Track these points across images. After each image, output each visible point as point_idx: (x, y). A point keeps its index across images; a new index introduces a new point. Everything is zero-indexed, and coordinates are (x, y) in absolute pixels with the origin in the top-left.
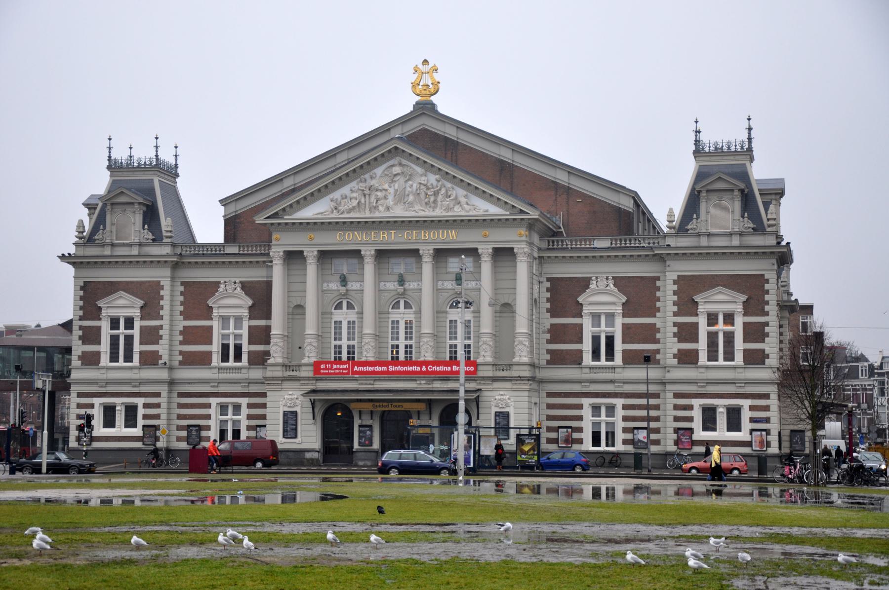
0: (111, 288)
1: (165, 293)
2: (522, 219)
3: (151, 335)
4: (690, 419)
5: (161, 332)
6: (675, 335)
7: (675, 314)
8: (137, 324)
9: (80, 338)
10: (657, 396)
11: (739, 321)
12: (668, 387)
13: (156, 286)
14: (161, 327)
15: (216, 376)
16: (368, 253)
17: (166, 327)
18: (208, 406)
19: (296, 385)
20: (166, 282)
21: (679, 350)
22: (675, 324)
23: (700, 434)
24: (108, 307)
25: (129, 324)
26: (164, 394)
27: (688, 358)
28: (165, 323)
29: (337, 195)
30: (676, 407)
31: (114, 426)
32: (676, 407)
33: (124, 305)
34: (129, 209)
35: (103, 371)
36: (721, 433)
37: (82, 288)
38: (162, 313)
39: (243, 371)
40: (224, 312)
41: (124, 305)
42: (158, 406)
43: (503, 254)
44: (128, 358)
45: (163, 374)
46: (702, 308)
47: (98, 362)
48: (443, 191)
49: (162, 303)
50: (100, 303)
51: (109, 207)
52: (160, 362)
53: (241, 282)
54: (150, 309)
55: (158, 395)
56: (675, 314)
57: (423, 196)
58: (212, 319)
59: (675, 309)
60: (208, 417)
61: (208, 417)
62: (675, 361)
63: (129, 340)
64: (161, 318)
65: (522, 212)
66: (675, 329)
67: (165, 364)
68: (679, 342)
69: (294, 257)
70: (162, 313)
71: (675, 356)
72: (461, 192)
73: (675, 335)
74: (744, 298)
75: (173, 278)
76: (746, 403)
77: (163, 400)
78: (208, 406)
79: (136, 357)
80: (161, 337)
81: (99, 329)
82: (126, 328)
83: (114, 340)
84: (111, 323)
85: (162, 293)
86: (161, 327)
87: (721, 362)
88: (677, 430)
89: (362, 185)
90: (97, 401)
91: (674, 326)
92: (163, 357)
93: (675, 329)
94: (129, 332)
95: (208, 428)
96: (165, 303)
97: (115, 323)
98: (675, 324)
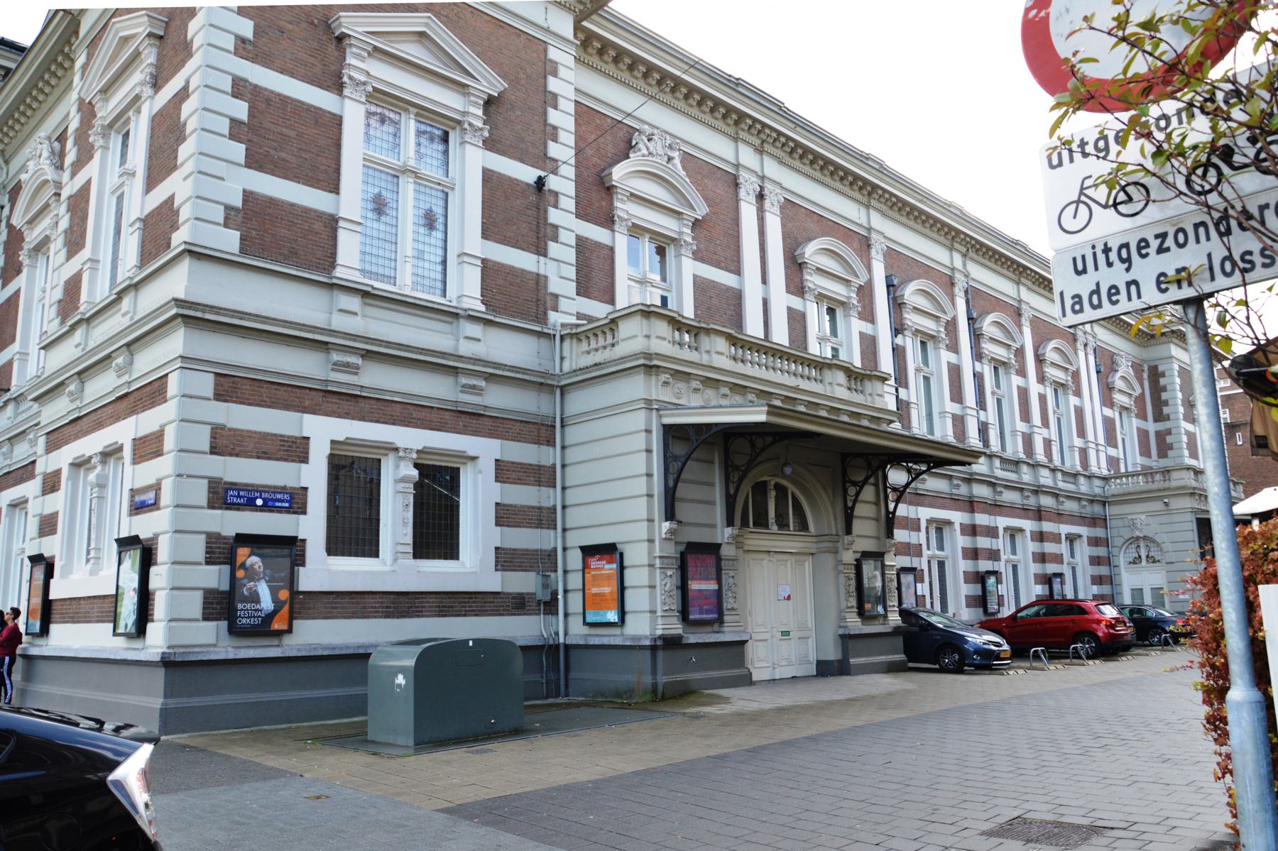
4: (295, 502)
6: (237, 130)
7: (243, 48)
21: (248, 196)
22: (240, 88)
23: (324, 571)
32: (224, 442)
36: (392, 565)
56: (243, 48)
62: (229, 241)
66: (241, 110)
68: (254, 162)
71: (231, 217)
73: (237, 130)
74: (489, 82)
76: (487, 449)
88: (222, 551)
91: (236, 94)
93: (241, 110)
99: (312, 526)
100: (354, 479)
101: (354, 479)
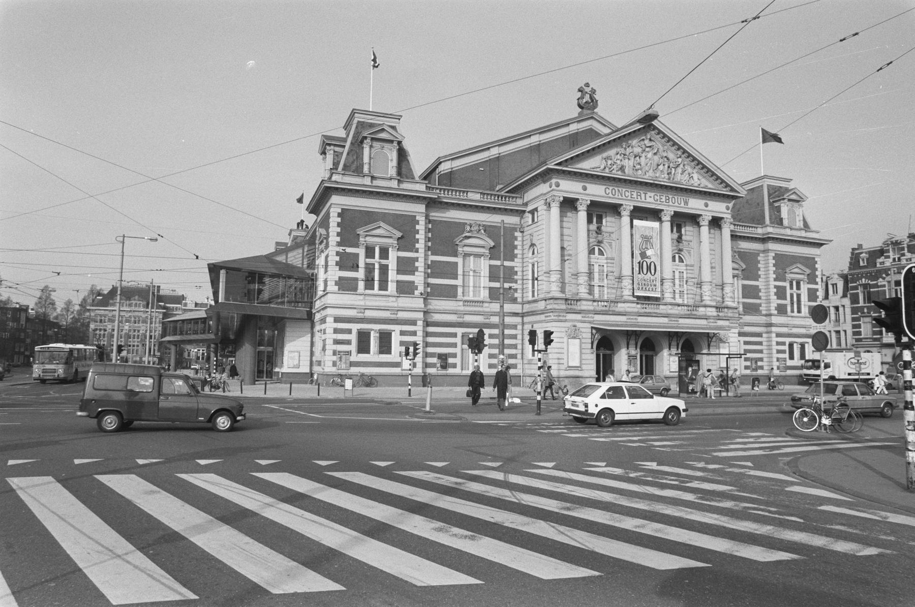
0: (370, 217)
1: (421, 227)
2: (733, 197)
3: (406, 266)
5: (417, 264)
7: (775, 280)
8: (393, 255)
9: (337, 264)
10: (759, 335)
11: (804, 287)
12: (774, 329)
13: (413, 220)
14: (417, 259)
15: (462, 308)
16: (628, 208)
17: (421, 260)
18: (454, 335)
19: (579, 317)
20: (421, 219)
22: (776, 287)
24: (367, 236)
25: (384, 253)
26: (420, 323)
27: (781, 310)
28: (421, 255)
29: (605, 155)
30: (778, 343)
31: (368, 352)
33: (382, 235)
34: (387, 145)
35: (362, 297)
37: (339, 215)
38: (417, 246)
39: (486, 305)
40: (467, 249)
41: (382, 235)
42: (414, 333)
43: (716, 223)
44: (384, 286)
45: (419, 303)
46: (789, 276)
47: (356, 289)
48: (681, 166)
49: (417, 236)
50: (361, 231)
51: (368, 140)
52: (417, 293)
53: (484, 226)
54: (406, 242)
55: (413, 322)
56: (775, 280)
57: (666, 166)
58: (456, 256)
59: (774, 276)
60: (454, 345)
61: (454, 345)
62: (776, 312)
63: (384, 269)
64: (417, 251)
65: (733, 190)
66: (775, 290)
67: (421, 294)
69: (569, 204)
70: (417, 246)
72: (689, 169)
75: (427, 217)
77: (419, 328)
78: (454, 335)
79: (392, 287)
80: (416, 269)
81: (357, 255)
82: (381, 258)
83: (369, 269)
84: (367, 252)
85: (417, 227)
86: (417, 259)
87: (795, 314)
89: (622, 151)
90: (355, 327)
92: (419, 288)
94: (384, 262)
95: (454, 355)
96: (421, 236)
97: (370, 252)
98: (776, 287)
99: (787, 355)
100: (791, 345)
101: (791, 345)
